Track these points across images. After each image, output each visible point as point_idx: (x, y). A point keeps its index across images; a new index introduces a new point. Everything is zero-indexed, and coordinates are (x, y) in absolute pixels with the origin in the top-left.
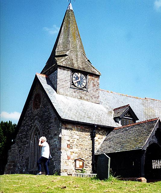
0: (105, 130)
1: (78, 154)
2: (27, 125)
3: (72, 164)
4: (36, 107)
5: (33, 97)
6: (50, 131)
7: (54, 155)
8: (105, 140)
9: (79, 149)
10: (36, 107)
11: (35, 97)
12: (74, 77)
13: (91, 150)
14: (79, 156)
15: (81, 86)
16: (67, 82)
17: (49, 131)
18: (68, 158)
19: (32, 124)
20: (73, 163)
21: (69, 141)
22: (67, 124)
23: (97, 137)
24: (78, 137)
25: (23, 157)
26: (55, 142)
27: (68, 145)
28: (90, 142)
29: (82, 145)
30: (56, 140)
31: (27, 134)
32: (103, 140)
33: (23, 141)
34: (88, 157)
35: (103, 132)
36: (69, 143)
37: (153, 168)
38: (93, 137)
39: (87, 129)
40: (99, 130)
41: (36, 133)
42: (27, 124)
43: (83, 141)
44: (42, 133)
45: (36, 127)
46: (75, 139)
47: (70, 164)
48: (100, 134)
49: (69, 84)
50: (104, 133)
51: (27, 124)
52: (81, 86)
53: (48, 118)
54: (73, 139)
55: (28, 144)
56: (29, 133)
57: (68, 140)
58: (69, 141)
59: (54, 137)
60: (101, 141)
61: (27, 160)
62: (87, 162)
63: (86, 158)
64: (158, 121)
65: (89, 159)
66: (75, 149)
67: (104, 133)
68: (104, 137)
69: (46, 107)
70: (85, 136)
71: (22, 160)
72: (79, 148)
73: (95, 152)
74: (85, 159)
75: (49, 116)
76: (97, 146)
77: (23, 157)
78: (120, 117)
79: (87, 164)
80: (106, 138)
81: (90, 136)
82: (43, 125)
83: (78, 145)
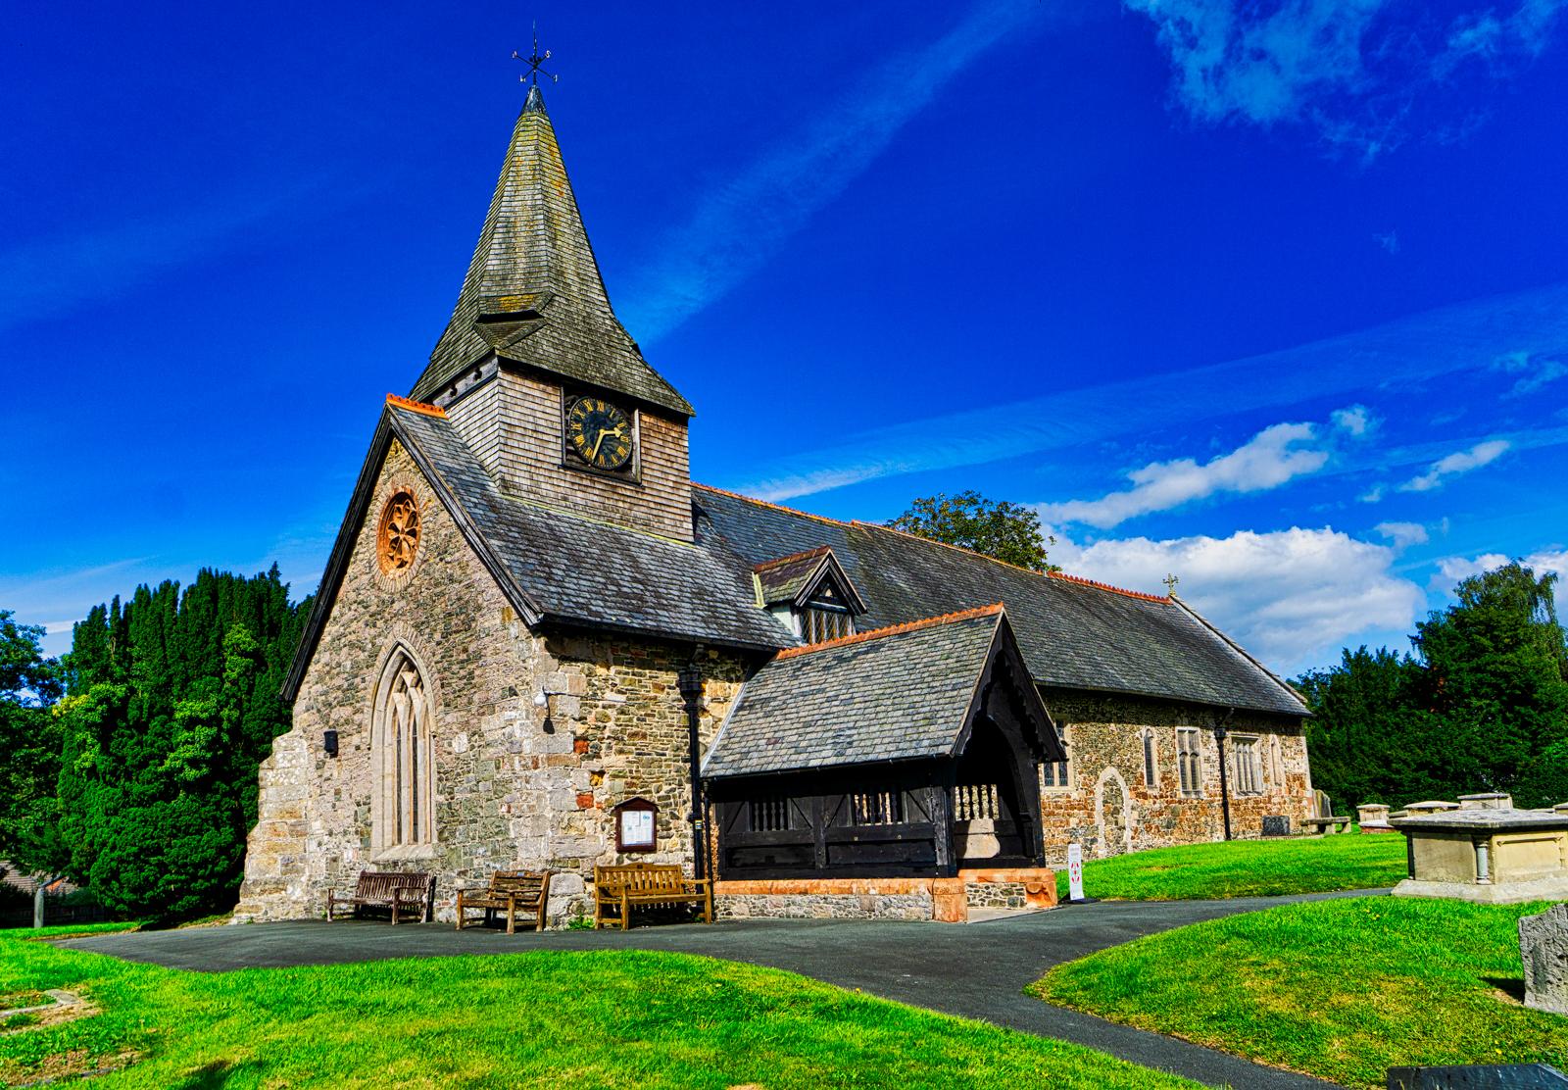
0: (736, 663)
1: (629, 780)
2: (351, 645)
3: (603, 829)
4: (392, 558)
5: (377, 508)
6: (477, 673)
7: (509, 791)
8: (740, 708)
9: (631, 757)
10: (392, 558)
11: (389, 511)
12: (577, 420)
13: (684, 754)
14: (633, 789)
15: (608, 460)
16: (545, 437)
17: (471, 673)
18: (578, 802)
19: (378, 641)
20: (606, 821)
21: (580, 719)
22: (566, 640)
23: (712, 688)
24: (623, 698)
25: (338, 792)
26: (508, 730)
27: (576, 740)
28: (675, 721)
29: (644, 736)
30: (515, 720)
31: (352, 687)
32: (735, 700)
33: (332, 716)
34: (674, 790)
35: (728, 671)
36: (580, 729)
37: (887, 795)
38: (691, 695)
39: (663, 658)
40: (713, 661)
41: (404, 683)
42: (350, 637)
43: (647, 715)
44: (438, 682)
45: (401, 653)
46: (609, 711)
47: (590, 831)
48: (716, 678)
49: (554, 453)
50: (733, 676)
51: (350, 637)
52: (608, 460)
53: (463, 609)
54: (600, 709)
55: (364, 734)
56: (363, 680)
57: (577, 716)
58: (580, 719)
59: (504, 703)
60: (724, 712)
61: (365, 808)
62: (668, 810)
63: (662, 793)
64: (999, 620)
65: (674, 797)
66: (612, 760)
67: (733, 676)
68: (736, 691)
69: (449, 559)
70: (652, 694)
71: (334, 806)
72: (631, 753)
73: (704, 763)
74: (659, 798)
75: (467, 602)
76: (711, 739)
77: (338, 792)
78: (797, 604)
79: (668, 823)
80: (745, 700)
81: (676, 693)
82: (438, 644)
83: (626, 738)
